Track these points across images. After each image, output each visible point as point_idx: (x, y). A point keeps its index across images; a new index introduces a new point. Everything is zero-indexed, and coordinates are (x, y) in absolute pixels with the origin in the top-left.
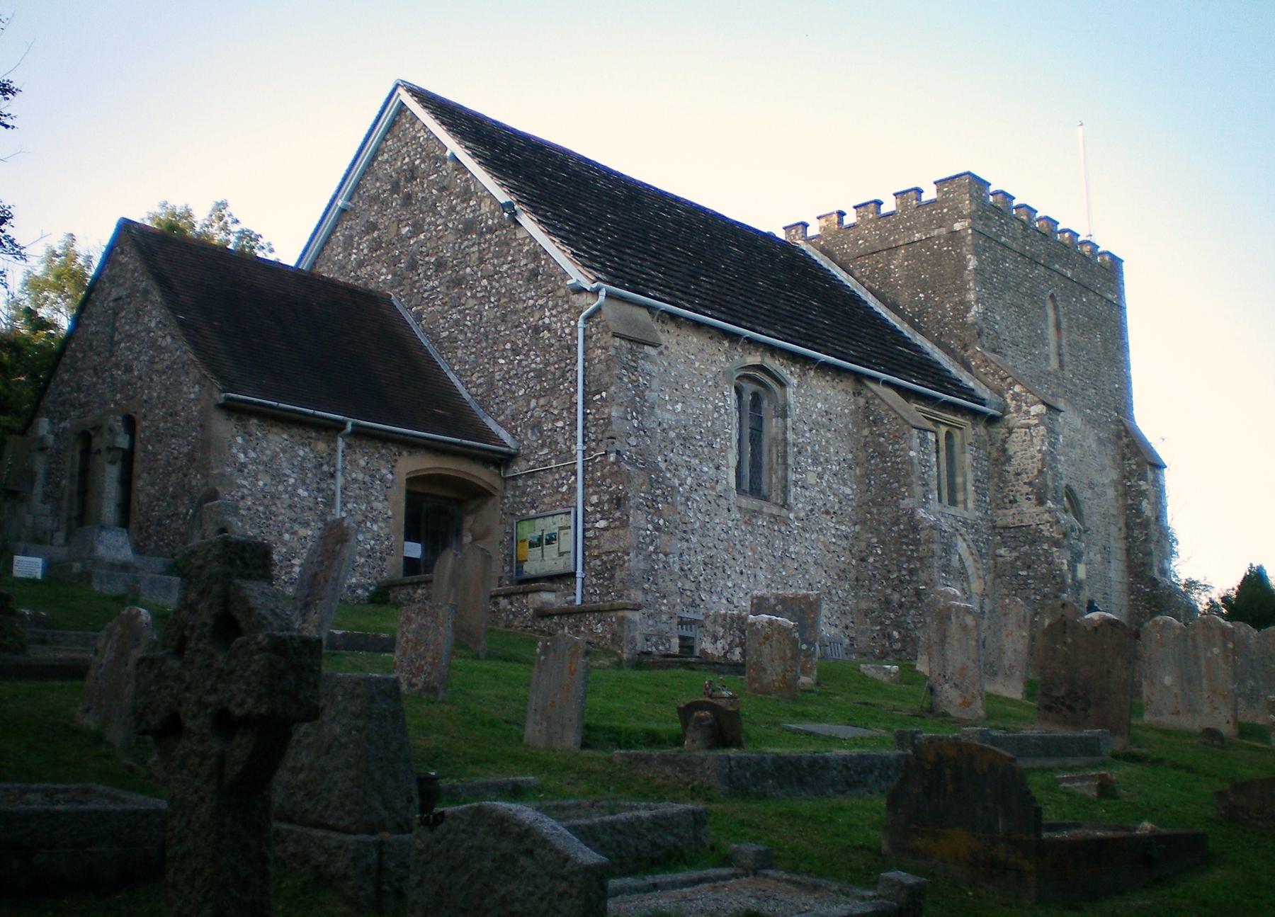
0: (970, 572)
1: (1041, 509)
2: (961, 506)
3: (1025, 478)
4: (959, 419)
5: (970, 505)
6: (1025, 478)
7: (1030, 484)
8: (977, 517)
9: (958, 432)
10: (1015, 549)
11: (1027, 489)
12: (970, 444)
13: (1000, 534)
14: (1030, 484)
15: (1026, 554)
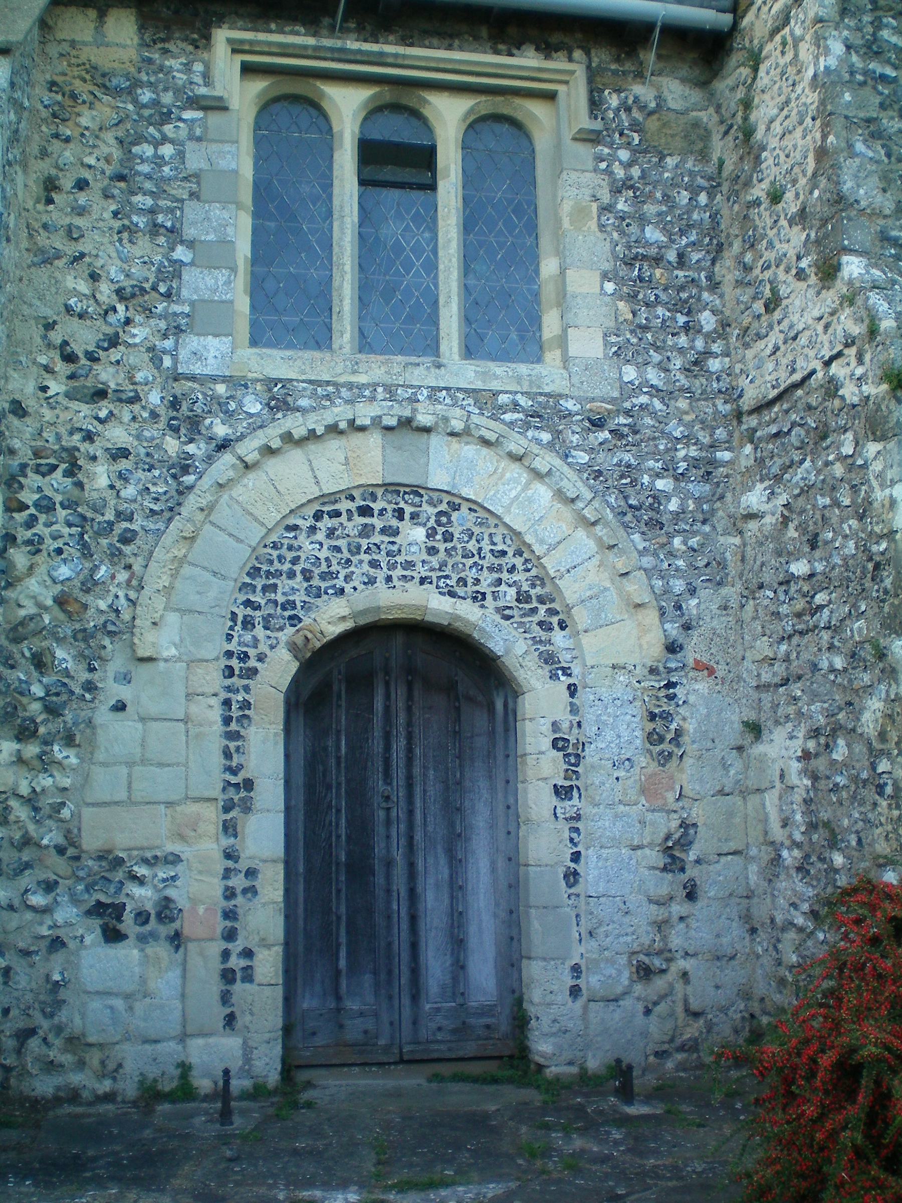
0: (571, 590)
1: (830, 297)
2: (552, 357)
3: (791, 204)
4: (528, 60)
5: (588, 344)
6: (791, 204)
7: (802, 217)
8: (629, 390)
9: (537, 109)
10: (778, 478)
11: (797, 237)
12: (592, 138)
13: (751, 436)
14: (802, 217)
15: (806, 490)
